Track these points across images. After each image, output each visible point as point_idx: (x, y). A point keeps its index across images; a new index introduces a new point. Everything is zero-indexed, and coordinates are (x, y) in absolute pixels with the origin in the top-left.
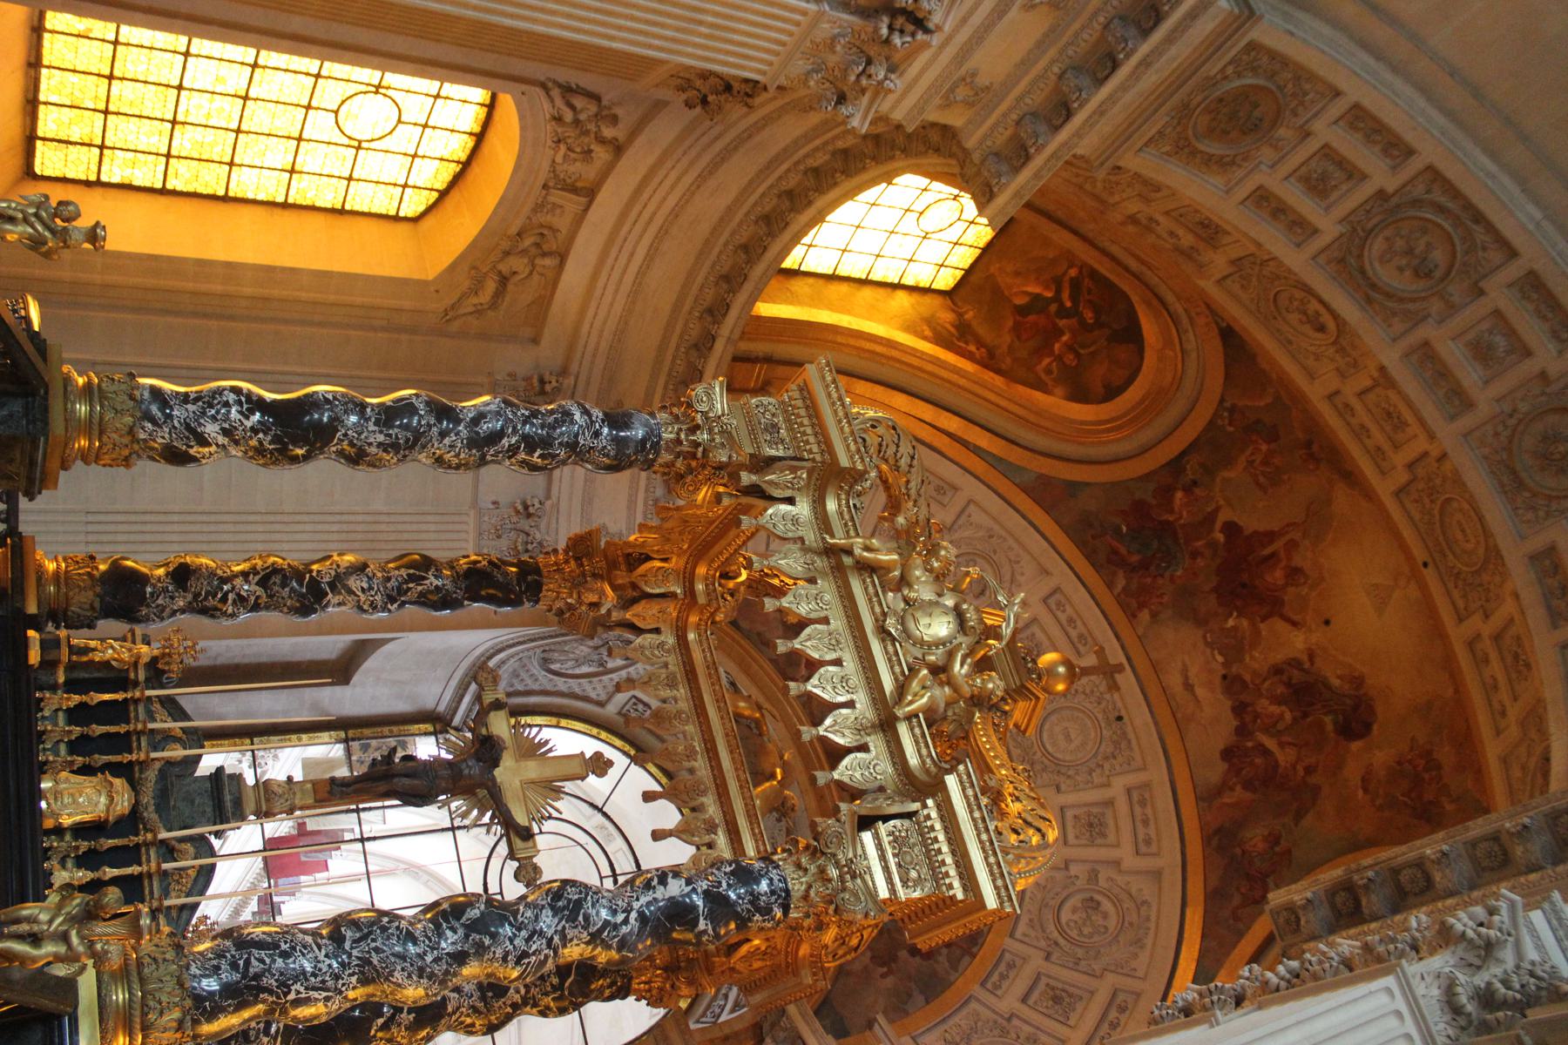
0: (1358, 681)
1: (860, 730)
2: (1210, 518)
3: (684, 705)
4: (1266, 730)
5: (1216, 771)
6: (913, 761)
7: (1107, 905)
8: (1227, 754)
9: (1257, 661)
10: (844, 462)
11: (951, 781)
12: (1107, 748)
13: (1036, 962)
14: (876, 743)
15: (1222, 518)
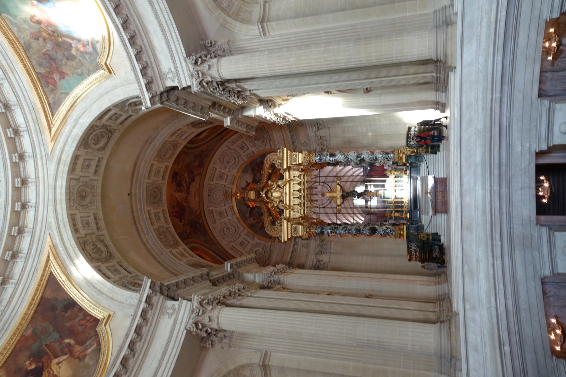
0: (172, 182)
1: (293, 180)
2: (184, 225)
3: (306, 203)
4: (187, 181)
5: (197, 178)
6: (287, 173)
7: (225, 161)
8: (193, 180)
9: (183, 195)
10: (286, 222)
11: (285, 167)
12: (213, 191)
13: (243, 155)
14: (292, 178)
15: (181, 224)
